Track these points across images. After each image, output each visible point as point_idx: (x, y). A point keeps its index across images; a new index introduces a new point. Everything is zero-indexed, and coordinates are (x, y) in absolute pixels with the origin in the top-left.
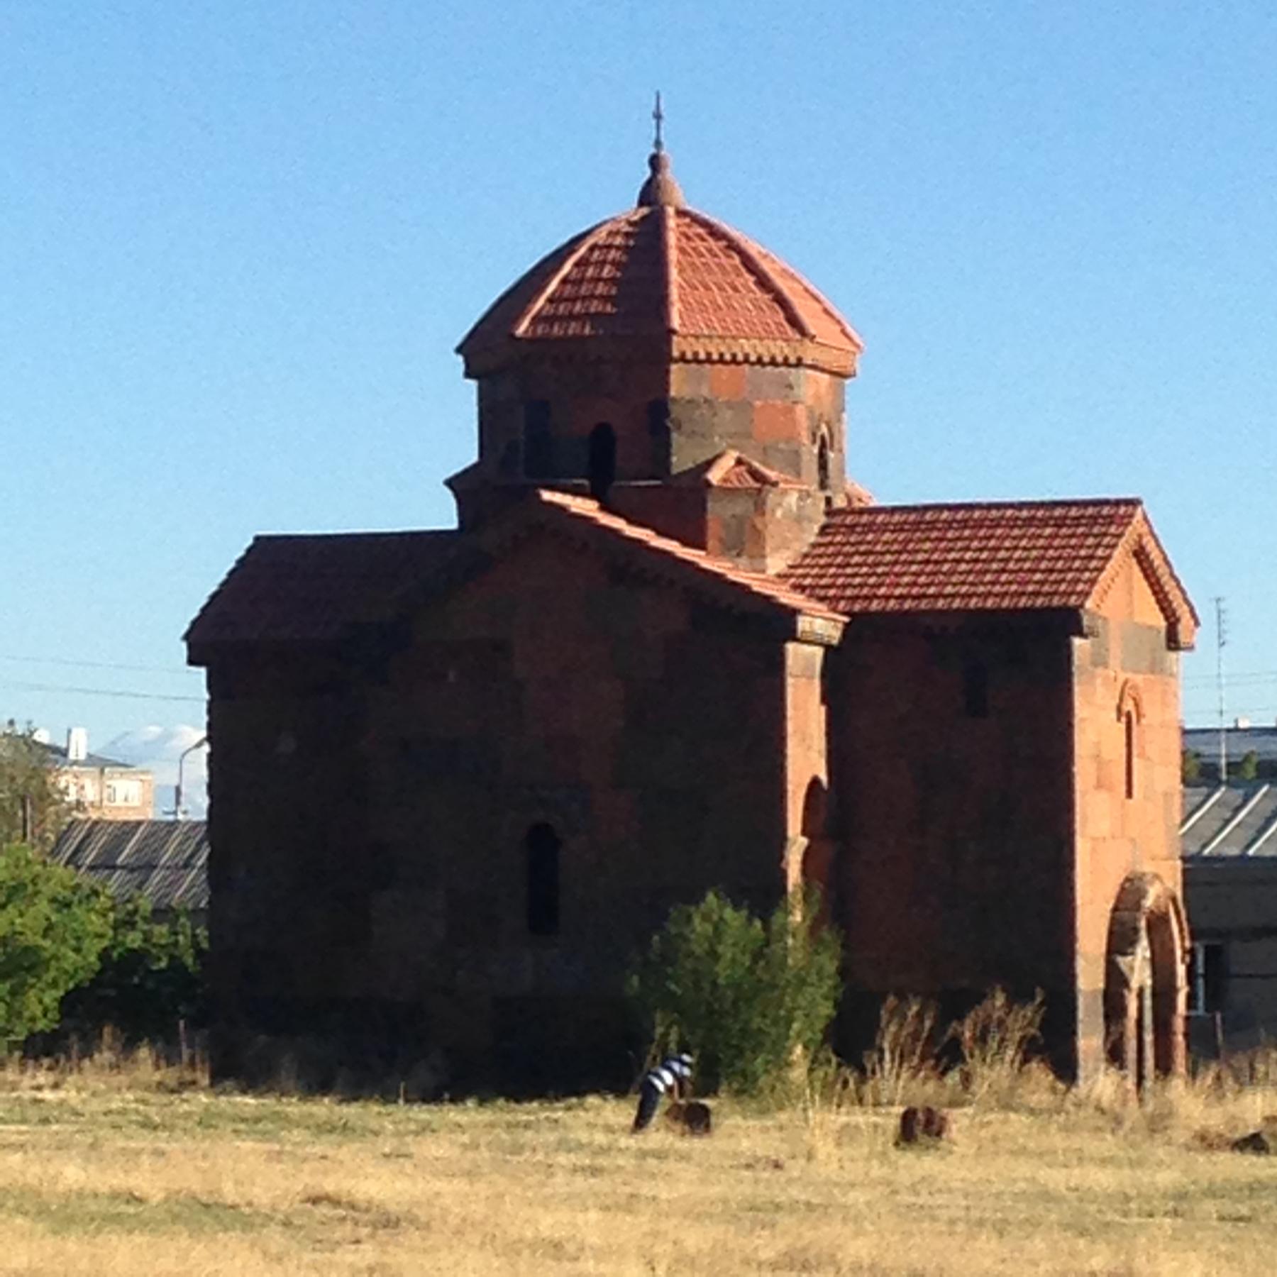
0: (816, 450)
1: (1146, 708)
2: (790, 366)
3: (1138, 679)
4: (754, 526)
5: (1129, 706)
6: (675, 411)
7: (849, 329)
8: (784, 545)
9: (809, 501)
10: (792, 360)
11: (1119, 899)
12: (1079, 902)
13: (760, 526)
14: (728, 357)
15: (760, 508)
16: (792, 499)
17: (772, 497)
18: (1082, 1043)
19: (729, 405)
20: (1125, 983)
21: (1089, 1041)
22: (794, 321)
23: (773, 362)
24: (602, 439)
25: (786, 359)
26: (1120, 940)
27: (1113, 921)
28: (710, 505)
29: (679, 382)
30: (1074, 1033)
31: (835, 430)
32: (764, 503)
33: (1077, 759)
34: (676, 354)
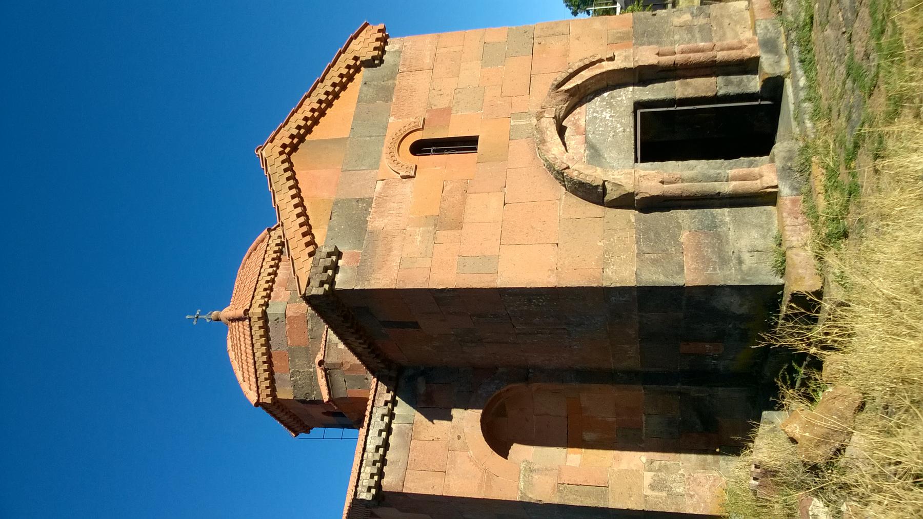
1: (412, 121)
4: (348, 370)
10: (261, 323)
11: (557, 178)
18: (690, 275)
19: (292, 361)
20: (631, 195)
23: (266, 336)
28: (342, 396)
29: (285, 393)
30: (680, 289)
32: (334, 364)
34: (268, 400)
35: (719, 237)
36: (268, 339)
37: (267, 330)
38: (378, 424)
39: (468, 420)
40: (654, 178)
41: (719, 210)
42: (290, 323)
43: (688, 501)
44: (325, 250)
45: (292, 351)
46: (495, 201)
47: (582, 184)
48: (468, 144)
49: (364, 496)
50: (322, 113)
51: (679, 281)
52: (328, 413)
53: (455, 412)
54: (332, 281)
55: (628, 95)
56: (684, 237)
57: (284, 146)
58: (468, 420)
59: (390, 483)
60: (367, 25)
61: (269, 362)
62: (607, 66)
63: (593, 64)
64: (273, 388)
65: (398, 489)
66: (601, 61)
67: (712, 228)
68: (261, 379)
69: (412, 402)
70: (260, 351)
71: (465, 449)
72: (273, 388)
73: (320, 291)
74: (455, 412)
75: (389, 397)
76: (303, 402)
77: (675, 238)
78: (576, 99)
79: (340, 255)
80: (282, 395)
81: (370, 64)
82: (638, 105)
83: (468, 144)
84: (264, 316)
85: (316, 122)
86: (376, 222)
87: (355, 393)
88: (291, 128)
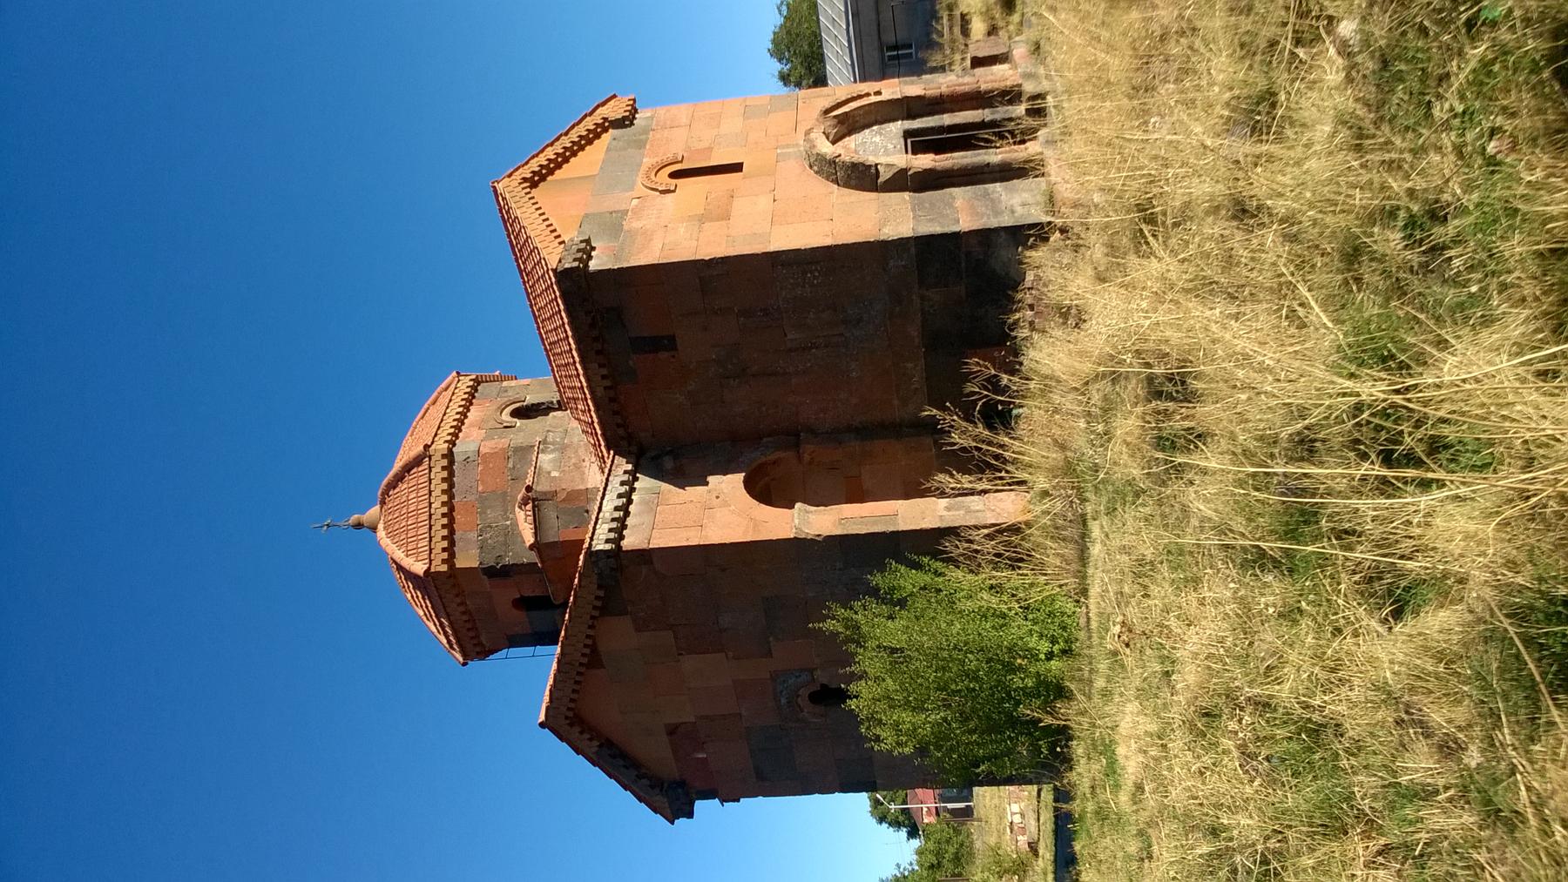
0: (519, 422)
1: (670, 156)
2: (452, 462)
3: (648, 161)
5: (663, 179)
6: (490, 561)
7: (443, 385)
8: (577, 467)
9: (550, 439)
10: (445, 462)
12: (828, 242)
13: (562, 496)
14: (445, 521)
15: (551, 496)
16: (546, 459)
17: (542, 487)
18: (965, 223)
20: (903, 171)
21: (962, 211)
22: (417, 461)
23: (449, 480)
24: (523, 603)
25: (444, 468)
26: (861, 177)
27: (847, 185)
29: (468, 559)
31: (512, 395)
32: (545, 493)
33: (698, 257)
34: (444, 568)
35: (992, 201)
36: (451, 486)
37: (451, 474)
38: (616, 488)
39: (730, 485)
40: (925, 161)
41: (991, 186)
42: (485, 462)
43: (989, 514)
44: (576, 240)
45: (482, 499)
46: (764, 202)
47: (855, 166)
48: (736, 168)
49: (599, 545)
50: (566, 160)
51: (956, 229)
52: (523, 603)
53: (710, 479)
54: (587, 266)
55: (897, 127)
56: (958, 203)
57: (525, 180)
58: (730, 485)
59: (630, 541)
60: (614, 96)
61: (449, 515)
62: (878, 98)
63: (860, 97)
64: (450, 550)
65: (645, 546)
66: (868, 95)
67: (986, 194)
68: (437, 538)
69: (658, 474)
70: (439, 499)
71: (726, 504)
72: (450, 550)
73: (576, 264)
74: (710, 479)
75: (630, 467)
76: (491, 572)
77: (951, 206)
78: (844, 129)
79: (593, 249)
80: (461, 563)
81: (620, 124)
82: (907, 134)
83: (736, 168)
84: (449, 456)
85: (559, 166)
86: (631, 224)
87: (570, 535)
88: (534, 165)
